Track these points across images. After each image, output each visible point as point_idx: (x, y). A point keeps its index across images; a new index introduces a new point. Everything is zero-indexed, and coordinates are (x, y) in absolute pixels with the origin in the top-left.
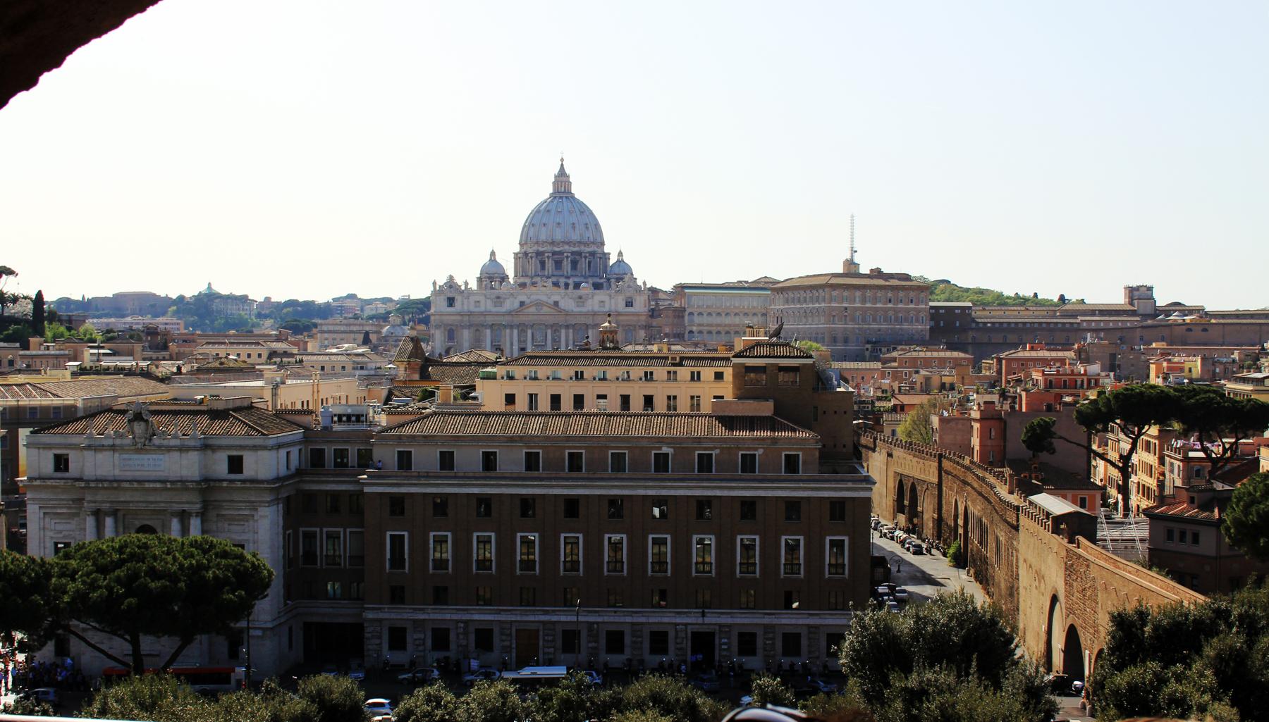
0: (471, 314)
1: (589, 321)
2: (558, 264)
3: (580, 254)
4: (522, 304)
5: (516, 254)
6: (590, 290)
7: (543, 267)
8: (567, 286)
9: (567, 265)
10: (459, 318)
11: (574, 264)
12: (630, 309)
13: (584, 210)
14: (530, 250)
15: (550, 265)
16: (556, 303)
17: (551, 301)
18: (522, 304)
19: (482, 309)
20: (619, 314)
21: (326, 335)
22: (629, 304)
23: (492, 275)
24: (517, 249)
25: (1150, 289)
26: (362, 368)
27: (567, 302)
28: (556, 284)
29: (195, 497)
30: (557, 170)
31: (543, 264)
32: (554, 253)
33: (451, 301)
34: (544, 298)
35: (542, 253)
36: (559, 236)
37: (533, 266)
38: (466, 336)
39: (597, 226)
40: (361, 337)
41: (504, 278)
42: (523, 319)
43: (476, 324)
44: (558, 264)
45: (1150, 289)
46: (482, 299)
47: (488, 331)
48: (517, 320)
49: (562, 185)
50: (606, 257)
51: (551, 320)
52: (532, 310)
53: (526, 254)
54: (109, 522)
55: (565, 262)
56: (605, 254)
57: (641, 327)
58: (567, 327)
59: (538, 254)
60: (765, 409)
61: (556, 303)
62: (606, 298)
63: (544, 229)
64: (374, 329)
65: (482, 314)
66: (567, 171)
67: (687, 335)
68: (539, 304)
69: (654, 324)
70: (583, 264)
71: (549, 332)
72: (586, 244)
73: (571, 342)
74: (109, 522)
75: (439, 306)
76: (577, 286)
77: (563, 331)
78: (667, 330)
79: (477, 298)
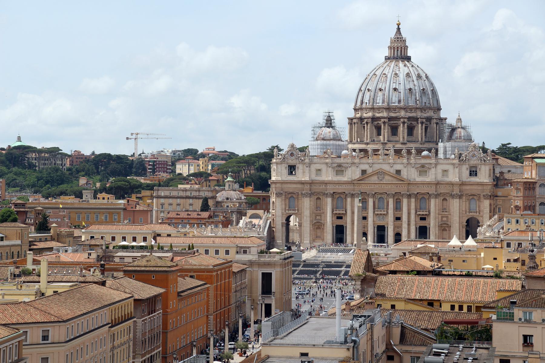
0: (312, 183)
1: (432, 190)
2: (394, 130)
3: (416, 119)
4: (364, 172)
5: (351, 119)
6: (433, 161)
7: (379, 134)
8: (409, 152)
9: (402, 131)
10: (299, 186)
11: (411, 130)
12: (474, 179)
14: (365, 115)
15: (386, 131)
16: (398, 172)
17: (392, 171)
18: (364, 172)
20: (462, 184)
21: (162, 201)
22: (473, 173)
24: (352, 114)
26: (245, 252)
27: (411, 174)
28: (398, 152)
30: (392, 33)
31: (378, 129)
32: (390, 119)
33: (292, 169)
34: (386, 167)
35: (379, 118)
37: (369, 131)
38: (306, 204)
39: (434, 92)
40: (198, 204)
42: (364, 188)
43: (316, 191)
44: (394, 130)
46: (323, 167)
47: (329, 200)
48: (357, 189)
51: (393, 190)
53: (361, 119)
55: (401, 129)
56: (441, 119)
57: (486, 197)
58: (409, 196)
59: (374, 119)
61: (398, 172)
62: (450, 168)
63: (380, 94)
64: (209, 194)
65: (326, 183)
66: (404, 34)
67: (537, 208)
68: (381, 173)
69: (500, 194)
70: (419, 130)
71: (391, 201)
72: (422, 109)
73: (413, 212)
75: (278, 174)
76: (419, 151)
77: (405, 201)
78: (519, 203)
79: (318, 166)
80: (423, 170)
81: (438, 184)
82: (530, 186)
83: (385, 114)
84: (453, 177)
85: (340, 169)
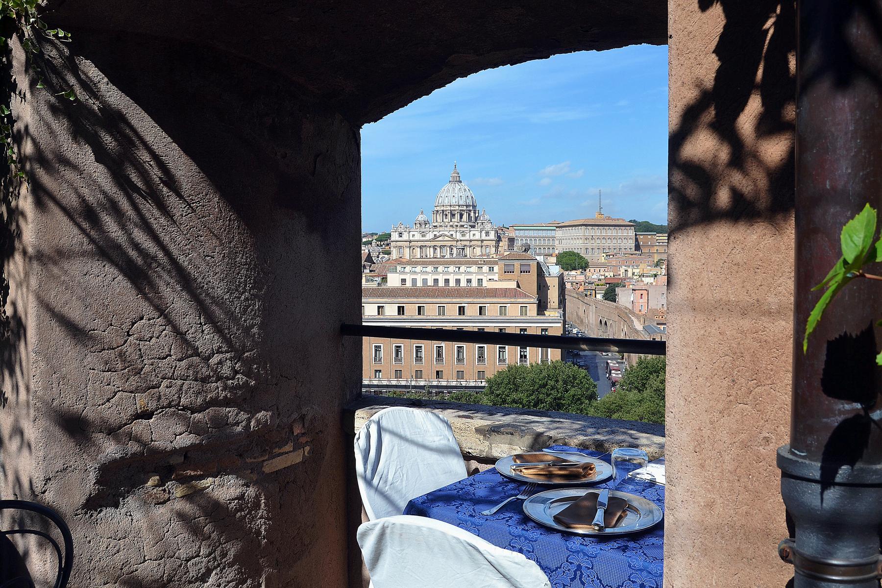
1: (468, 243)
15: (449, 216)
19: (416, 238)
22: (487, 233)
33: (400, 235)
34: (446, 233)
36: (454, 201)
48: (433, 244)
51: (449, 244)
60: (513, 285)
75: (395, 236)
83: (449, 208)
84: (477, 237)
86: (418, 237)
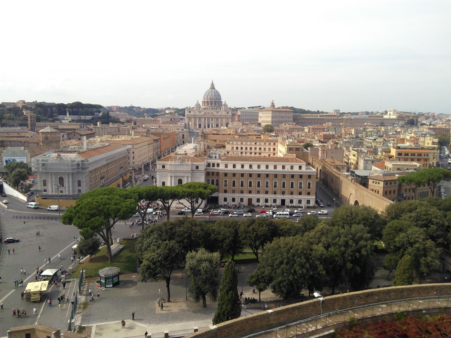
1: (219, 117)
2: (212, 104)
9: (213, 104)
11: (215, 104)
13: (218, 93)
15: (210, 104)
20: (226, 116)
22: (228, 113)
23: (198, 105)
25: (339, 110)
27: (215, 113)
29: (190, 174)
33: (190, 112)
34: (210, 112)
38: (193, 120)
41: (200, 107)
44: (212, 104)
45: (339, 110)
49: (213, 87)
50: (222, 102)
52: (207, 114)
54: (173, 178)
68: (209, 113)
74: (173, 178)
76: (217, 109)
80: (217, 112)
81: (220, 115)
82: (239, 116)
85: (200, 112)
86: (197, 113)
